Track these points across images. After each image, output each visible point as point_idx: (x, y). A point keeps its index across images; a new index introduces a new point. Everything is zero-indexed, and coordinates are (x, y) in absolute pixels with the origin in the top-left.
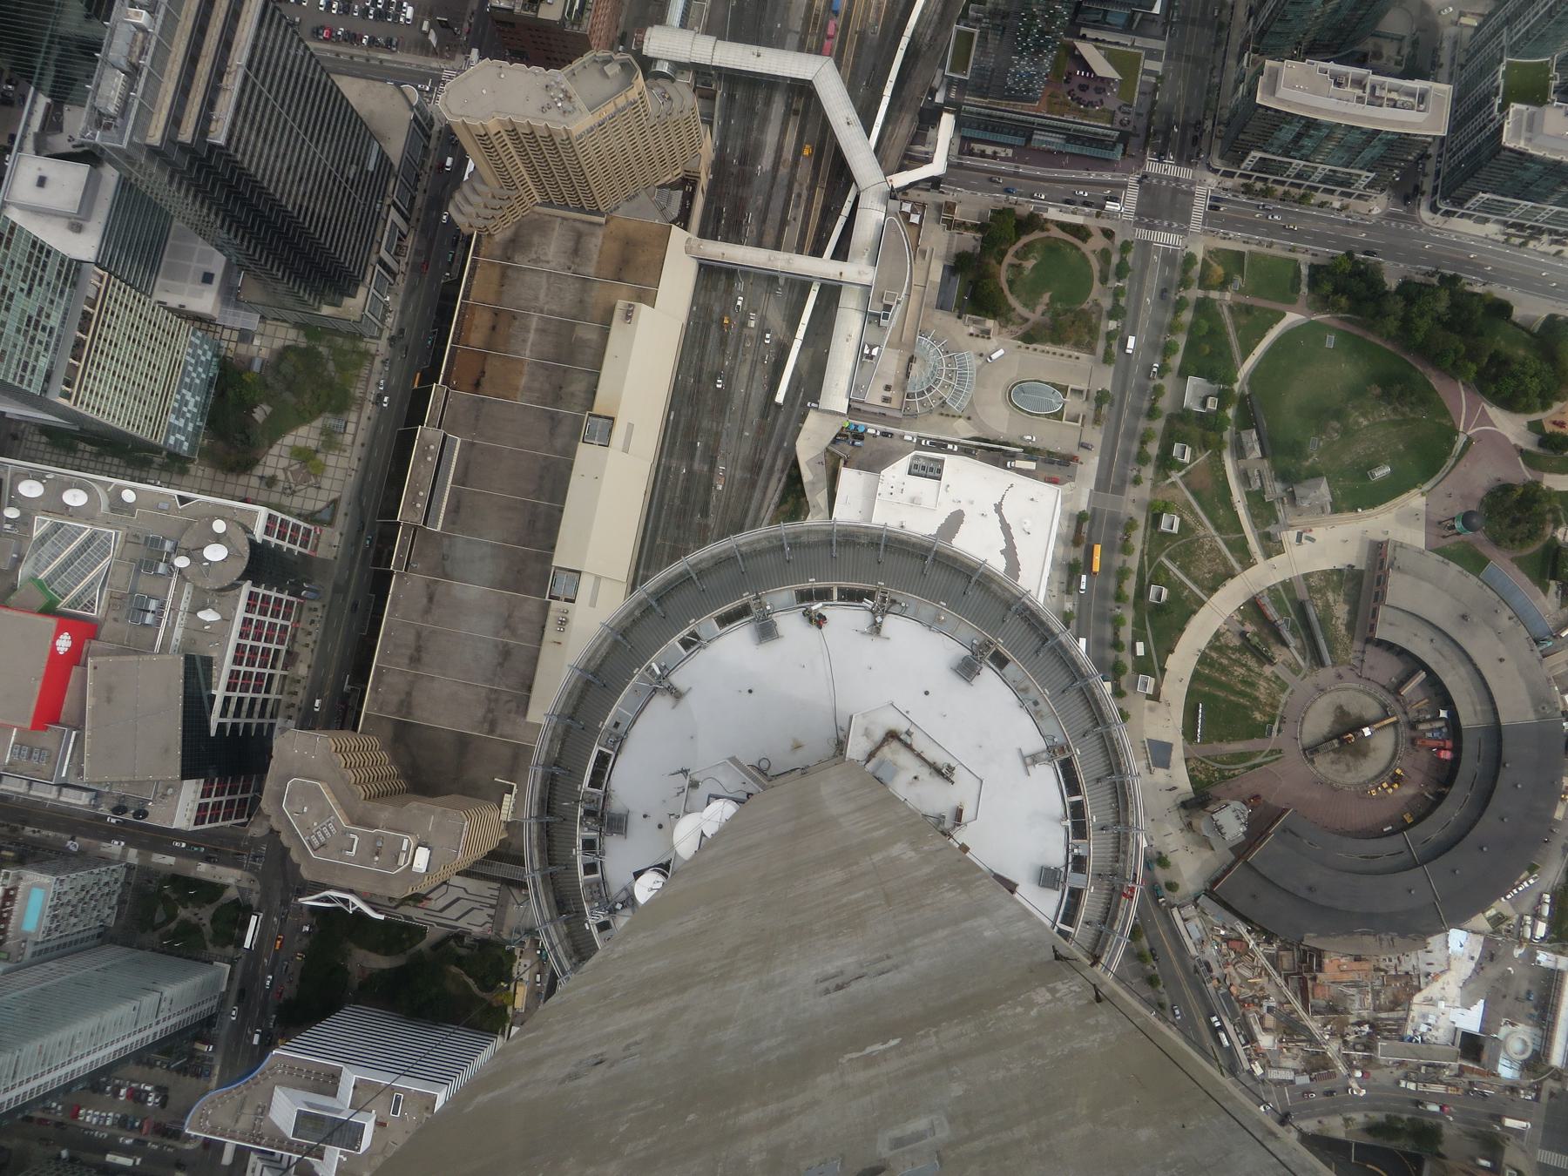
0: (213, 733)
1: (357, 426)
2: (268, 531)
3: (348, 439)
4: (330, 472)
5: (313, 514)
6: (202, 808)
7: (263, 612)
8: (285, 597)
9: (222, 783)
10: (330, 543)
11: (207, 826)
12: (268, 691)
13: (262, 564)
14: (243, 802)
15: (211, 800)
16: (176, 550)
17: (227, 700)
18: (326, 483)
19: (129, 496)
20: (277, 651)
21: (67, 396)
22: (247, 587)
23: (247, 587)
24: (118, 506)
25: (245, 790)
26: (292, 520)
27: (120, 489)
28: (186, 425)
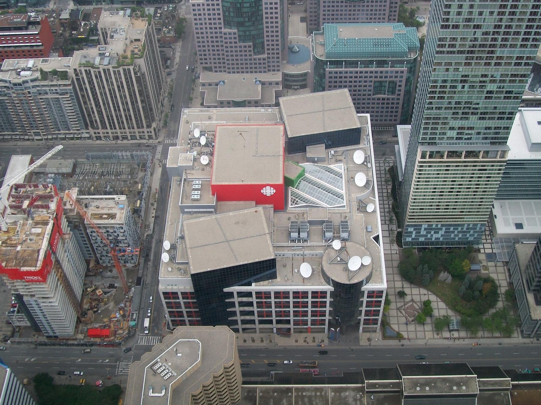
0: (226, 290)
1: (457, 340)
2: (371, 294)
3: (446, 334)
4: (420, 328)
5: (389, 324)
6: (174, 295)
7: (314, 304)
8: (327, 318)
9: (194, 305)
10: (370, 339)
11: (164, 301)
12: (261, 322)
13: (347, 294)
14: (180, 314)
15: (181, 301)
16: (344, 240)
17: (249, 294)
18: (411, 327)
19: (370, 208)
20: (288, 322)
21: (423, 156)
22: (329, 288)
23: (329, 288)
24: (362, 207)
25: (189, 314)
26: (381, 309)
27: (373, 202)
28: (422, 236)
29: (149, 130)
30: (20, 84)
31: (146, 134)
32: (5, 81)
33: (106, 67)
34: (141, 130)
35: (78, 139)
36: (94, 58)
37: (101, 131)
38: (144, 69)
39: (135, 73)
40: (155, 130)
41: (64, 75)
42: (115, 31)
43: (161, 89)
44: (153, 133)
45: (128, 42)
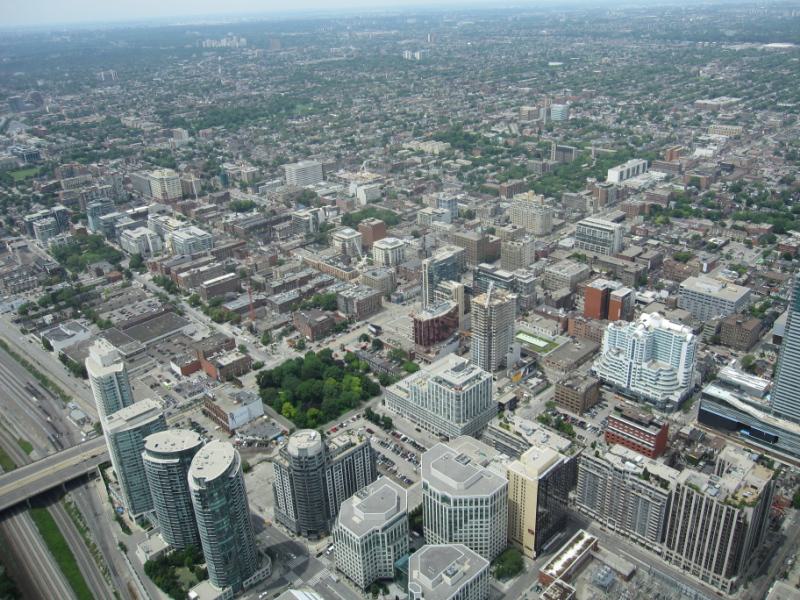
29: (726, 580)
30: (620, 472)
31: (721, 583)
32: (609, 462)
33: (711, 498)
34: (717, 576)
35: (648, 548)
36: (702, 484)
37: (675, 553)
38: (749, 519)
39: (739, 518)
40: (732, 584)
41: (665, 484)
42: (735, 469)
43: (756, 546)
44: (729, 587)
45: (743, 484)
